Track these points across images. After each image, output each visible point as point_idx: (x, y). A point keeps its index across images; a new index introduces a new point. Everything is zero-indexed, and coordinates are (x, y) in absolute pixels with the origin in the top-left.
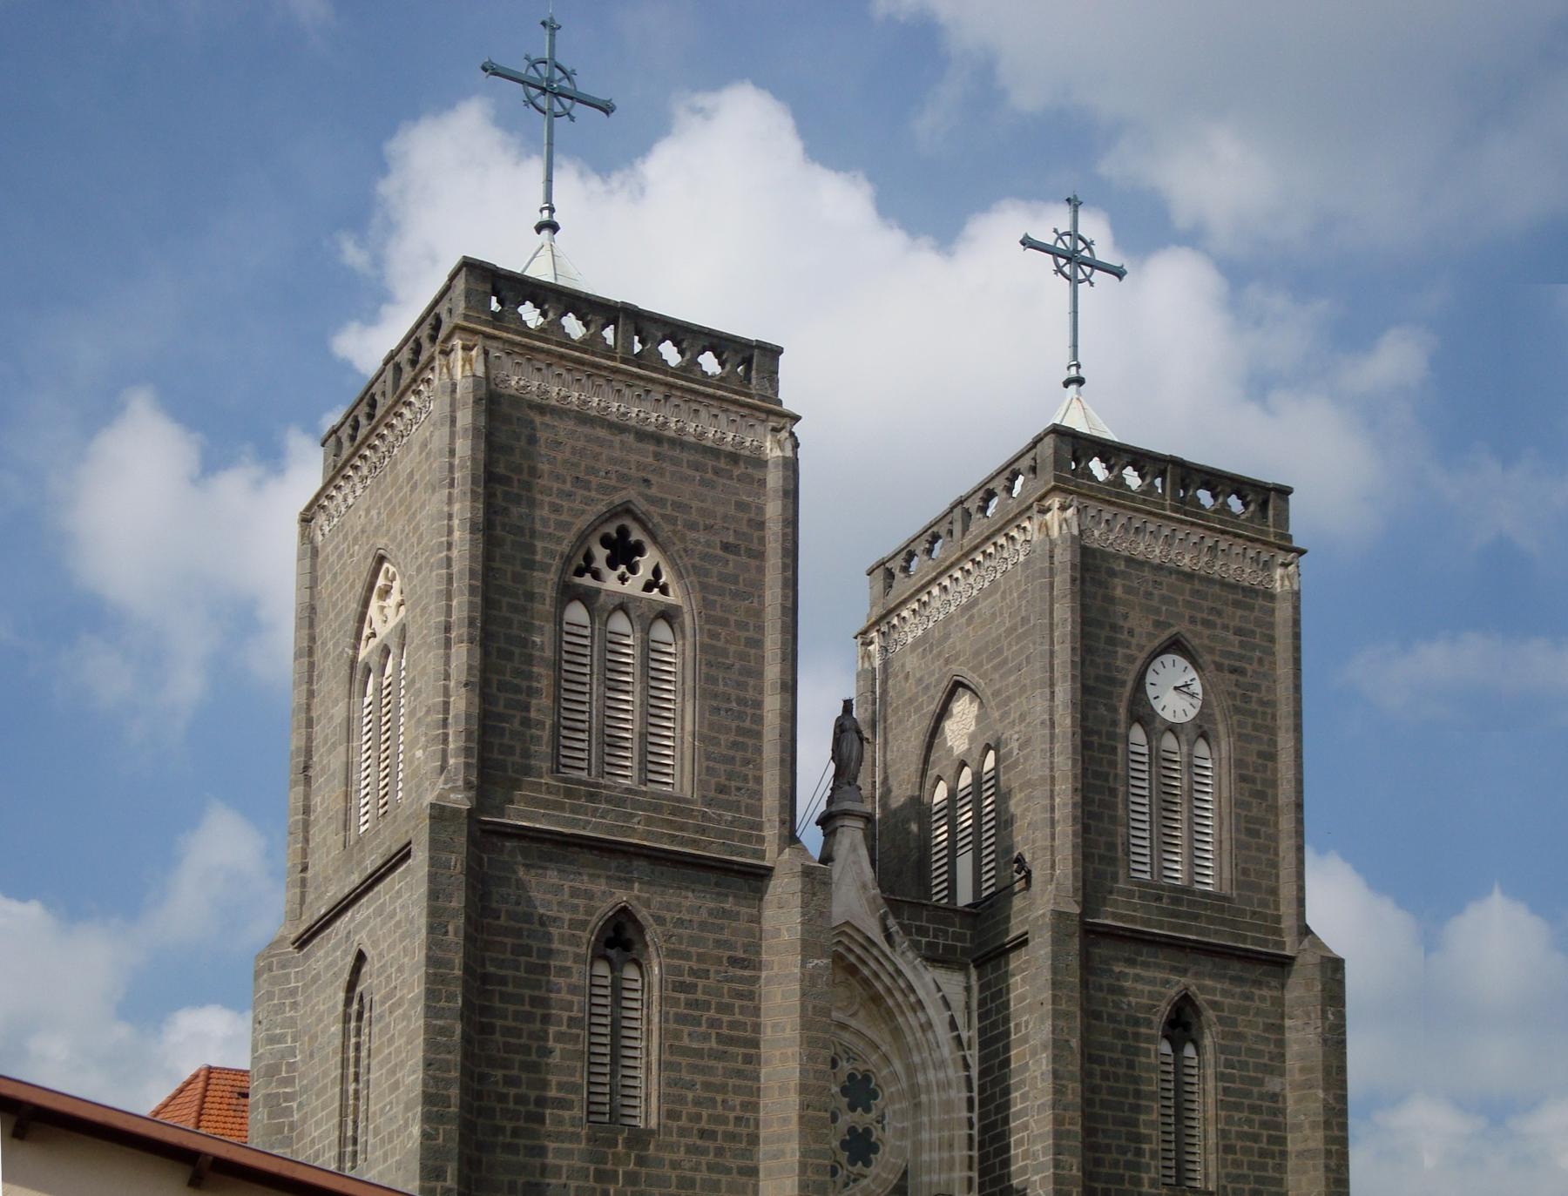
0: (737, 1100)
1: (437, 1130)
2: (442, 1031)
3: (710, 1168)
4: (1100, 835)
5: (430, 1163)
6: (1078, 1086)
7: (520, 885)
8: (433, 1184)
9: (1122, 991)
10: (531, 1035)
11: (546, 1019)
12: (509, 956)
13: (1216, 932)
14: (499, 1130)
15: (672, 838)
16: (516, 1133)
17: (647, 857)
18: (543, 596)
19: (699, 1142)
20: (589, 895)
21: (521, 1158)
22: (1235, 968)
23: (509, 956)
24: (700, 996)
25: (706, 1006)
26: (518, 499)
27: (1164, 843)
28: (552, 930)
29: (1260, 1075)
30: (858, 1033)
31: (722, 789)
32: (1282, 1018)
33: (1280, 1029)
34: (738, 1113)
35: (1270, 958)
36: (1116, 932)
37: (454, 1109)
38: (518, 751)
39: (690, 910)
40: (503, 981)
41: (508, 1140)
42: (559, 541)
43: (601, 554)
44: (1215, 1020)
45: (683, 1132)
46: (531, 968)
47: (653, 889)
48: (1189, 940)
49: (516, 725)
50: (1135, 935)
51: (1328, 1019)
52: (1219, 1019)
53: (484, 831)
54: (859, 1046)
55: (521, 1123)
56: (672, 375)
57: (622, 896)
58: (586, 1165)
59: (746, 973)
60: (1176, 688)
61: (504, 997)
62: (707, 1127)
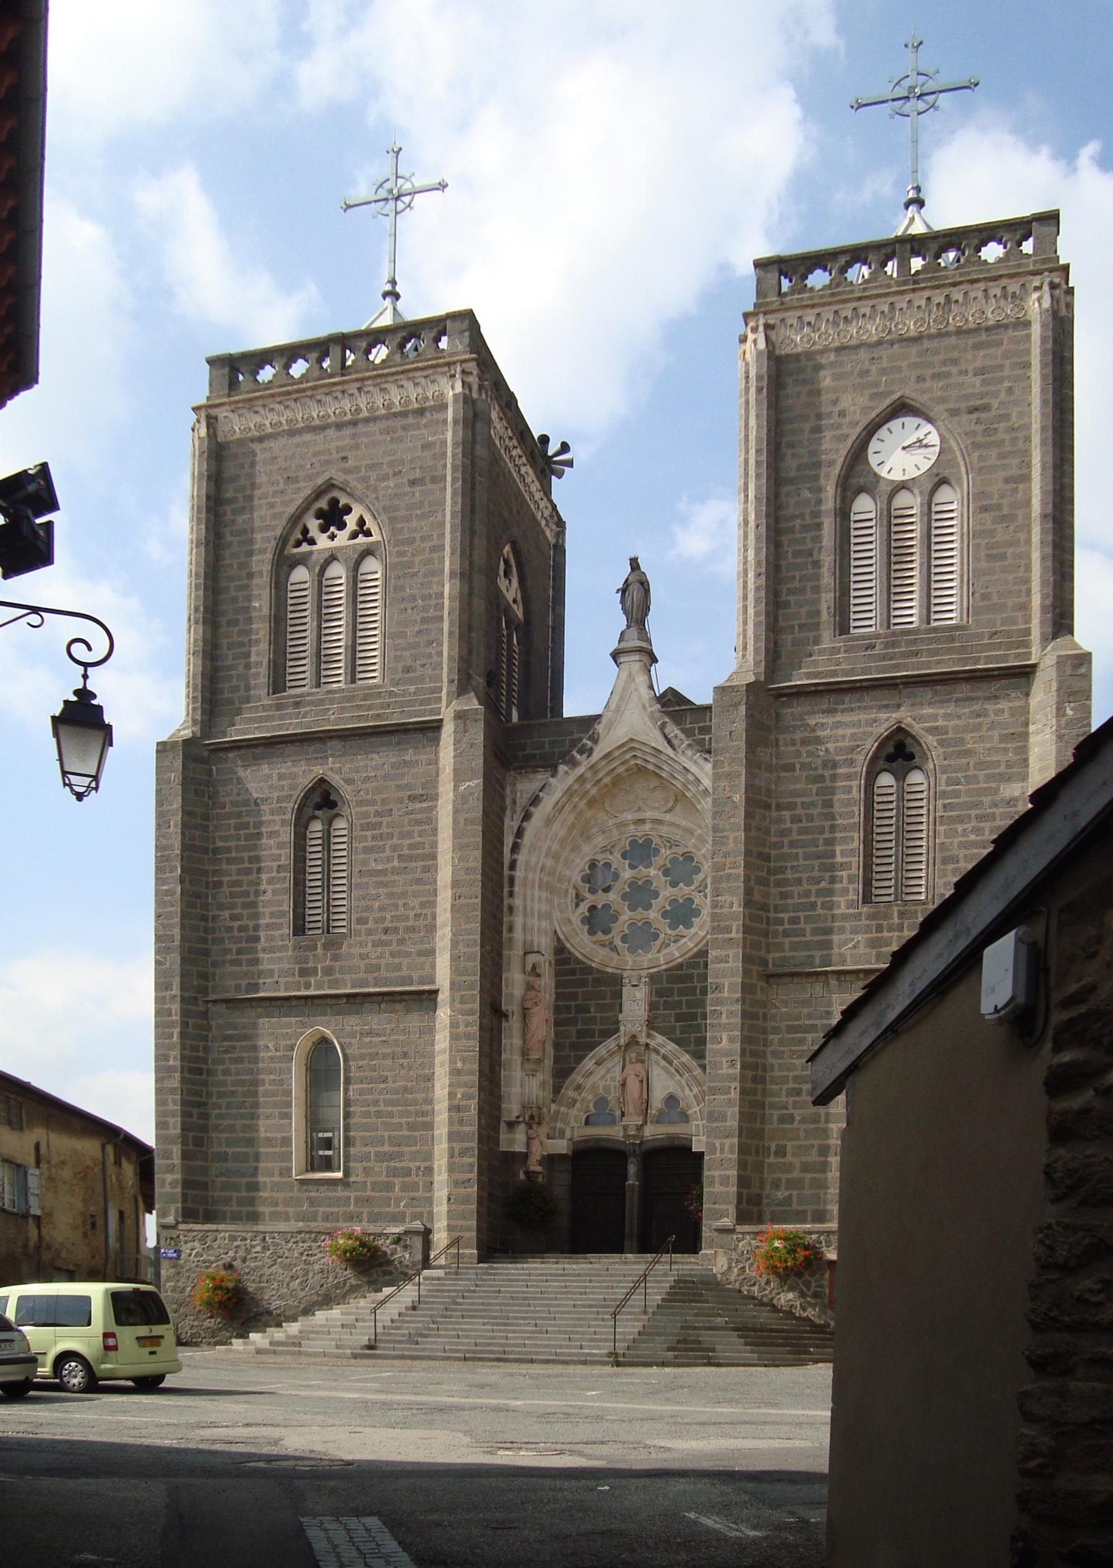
0: (414, 902)
1: (165, 958)
2: (167, 893)
3: (392, 955)
4: (801, 607)
5: (162, 980)
6: (741, 834)
7: (239, 781)
8: (163, 994)
9: (818, 741)
10: (250, 883)
11: (259, 870)
12: (232, 832)
13: (939, 662)
14: (227, 951)
15: (360, 718)
16: (239, 952)
17: (339, 737)
18: (261, 573)
19: (384, 937)
20: (294, 776)
21: (244, 968)
22: (963, 690)
23: (232, 832)
24: (385, 830)
25: (391, 836)
26: (242, 510)
27: (891, 593)
28: (262, 807)
29: (993, 785)
30: (672, 824)
31: (407, 670)
32: (1027, 724)
33: (1025, 736)
34: (418, 911)
35: (1002, 672)
36: (808, 689)
37: (177, 943)
38: (242, 688)
39: (375, 768)
40: (228, 850)
41: (235, 957)
42: (273, 528)
43: (313, 524)
44: (935, 744)
45: (369, 932)
46: (248, 838)
47: (343, 759)
48: (410, 723)
49: (241, 669)
50: (830, 687)
51: (1064, 715)
52: (941, 743)
53: (211, 751)
54: (677, 835)
55: (244, 945)
56: (382, 368)
57: (319, 771)
58: (292, 966)
59: (424, 805)
60: (904, 448)
61: (229, 861)
62: (390, 925)
